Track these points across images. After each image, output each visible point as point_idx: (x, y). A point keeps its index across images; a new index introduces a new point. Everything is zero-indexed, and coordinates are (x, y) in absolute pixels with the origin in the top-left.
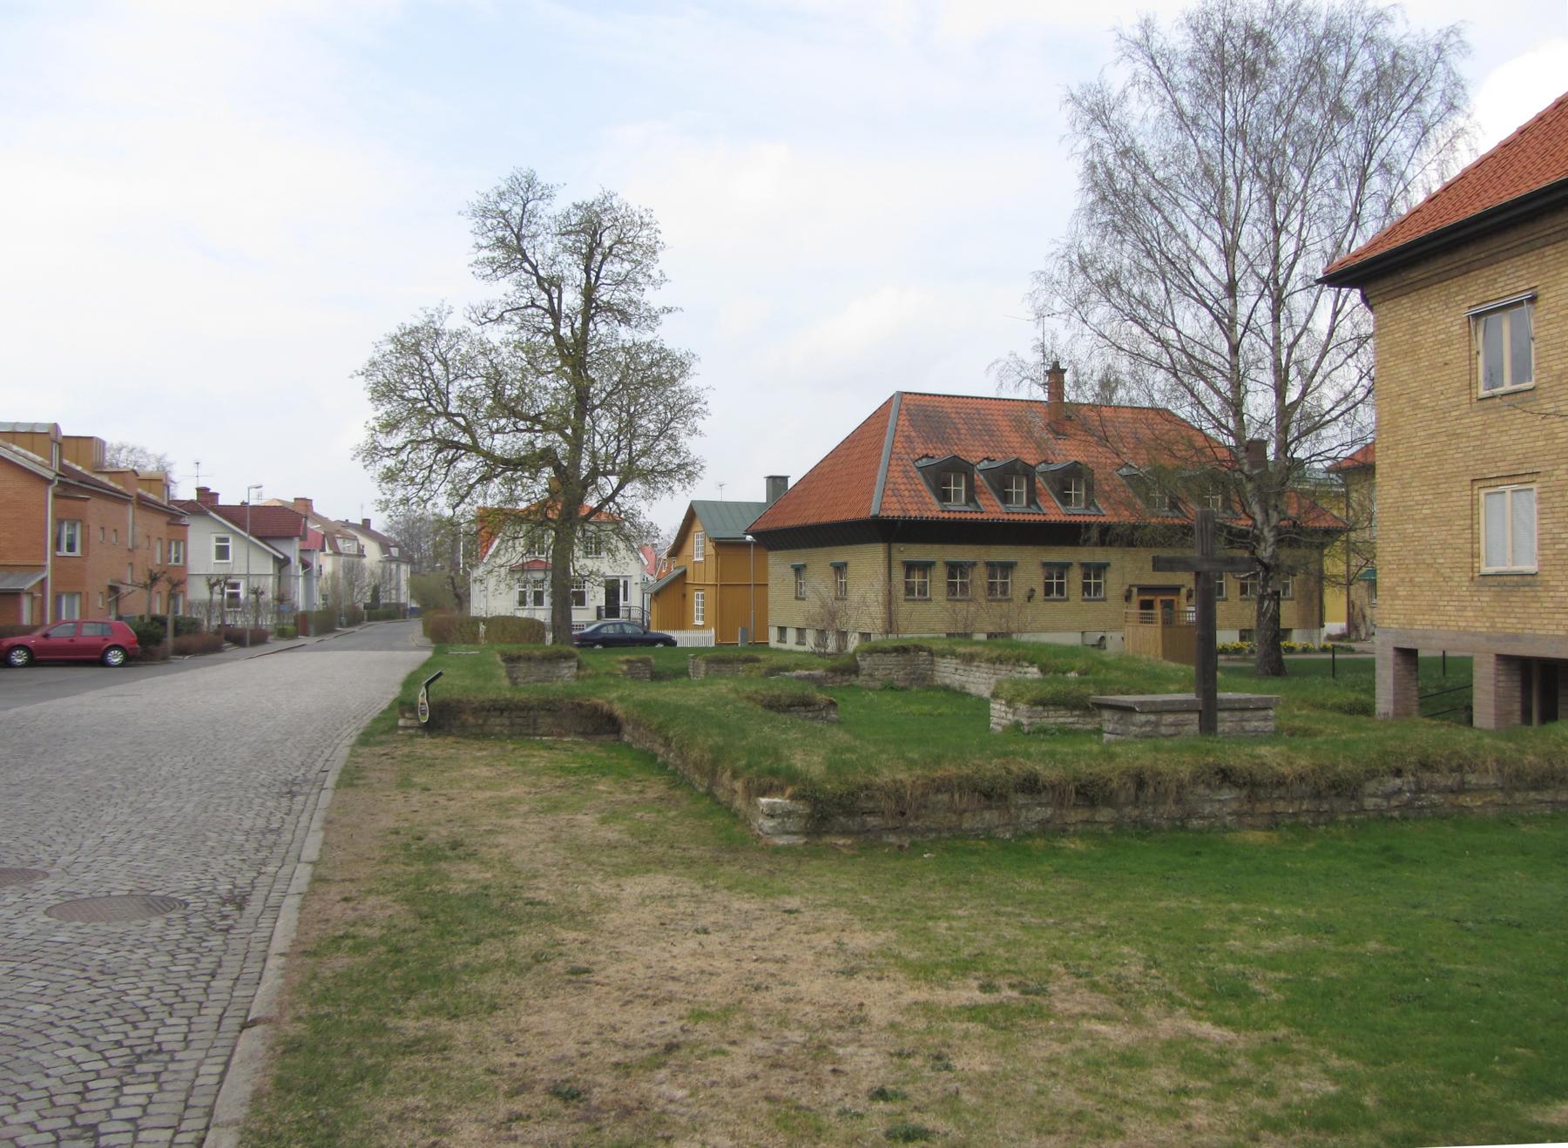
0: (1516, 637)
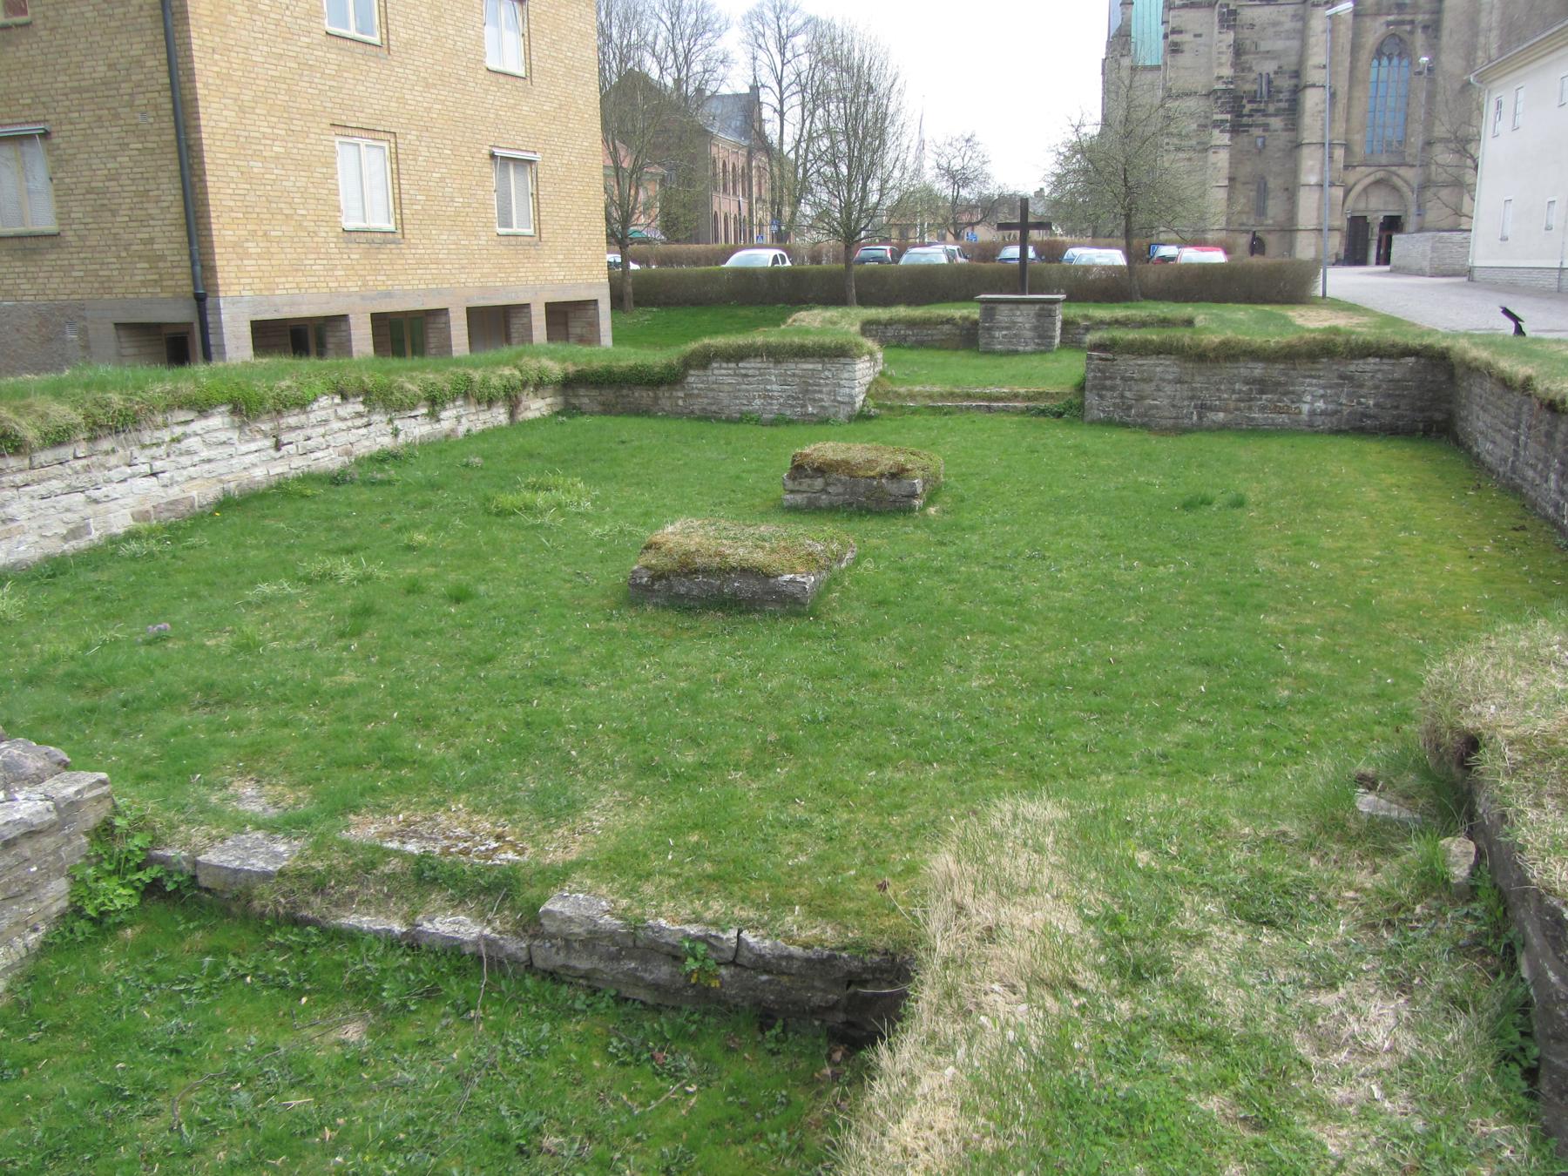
0: (388, 295)
